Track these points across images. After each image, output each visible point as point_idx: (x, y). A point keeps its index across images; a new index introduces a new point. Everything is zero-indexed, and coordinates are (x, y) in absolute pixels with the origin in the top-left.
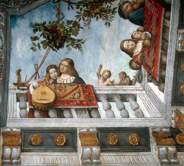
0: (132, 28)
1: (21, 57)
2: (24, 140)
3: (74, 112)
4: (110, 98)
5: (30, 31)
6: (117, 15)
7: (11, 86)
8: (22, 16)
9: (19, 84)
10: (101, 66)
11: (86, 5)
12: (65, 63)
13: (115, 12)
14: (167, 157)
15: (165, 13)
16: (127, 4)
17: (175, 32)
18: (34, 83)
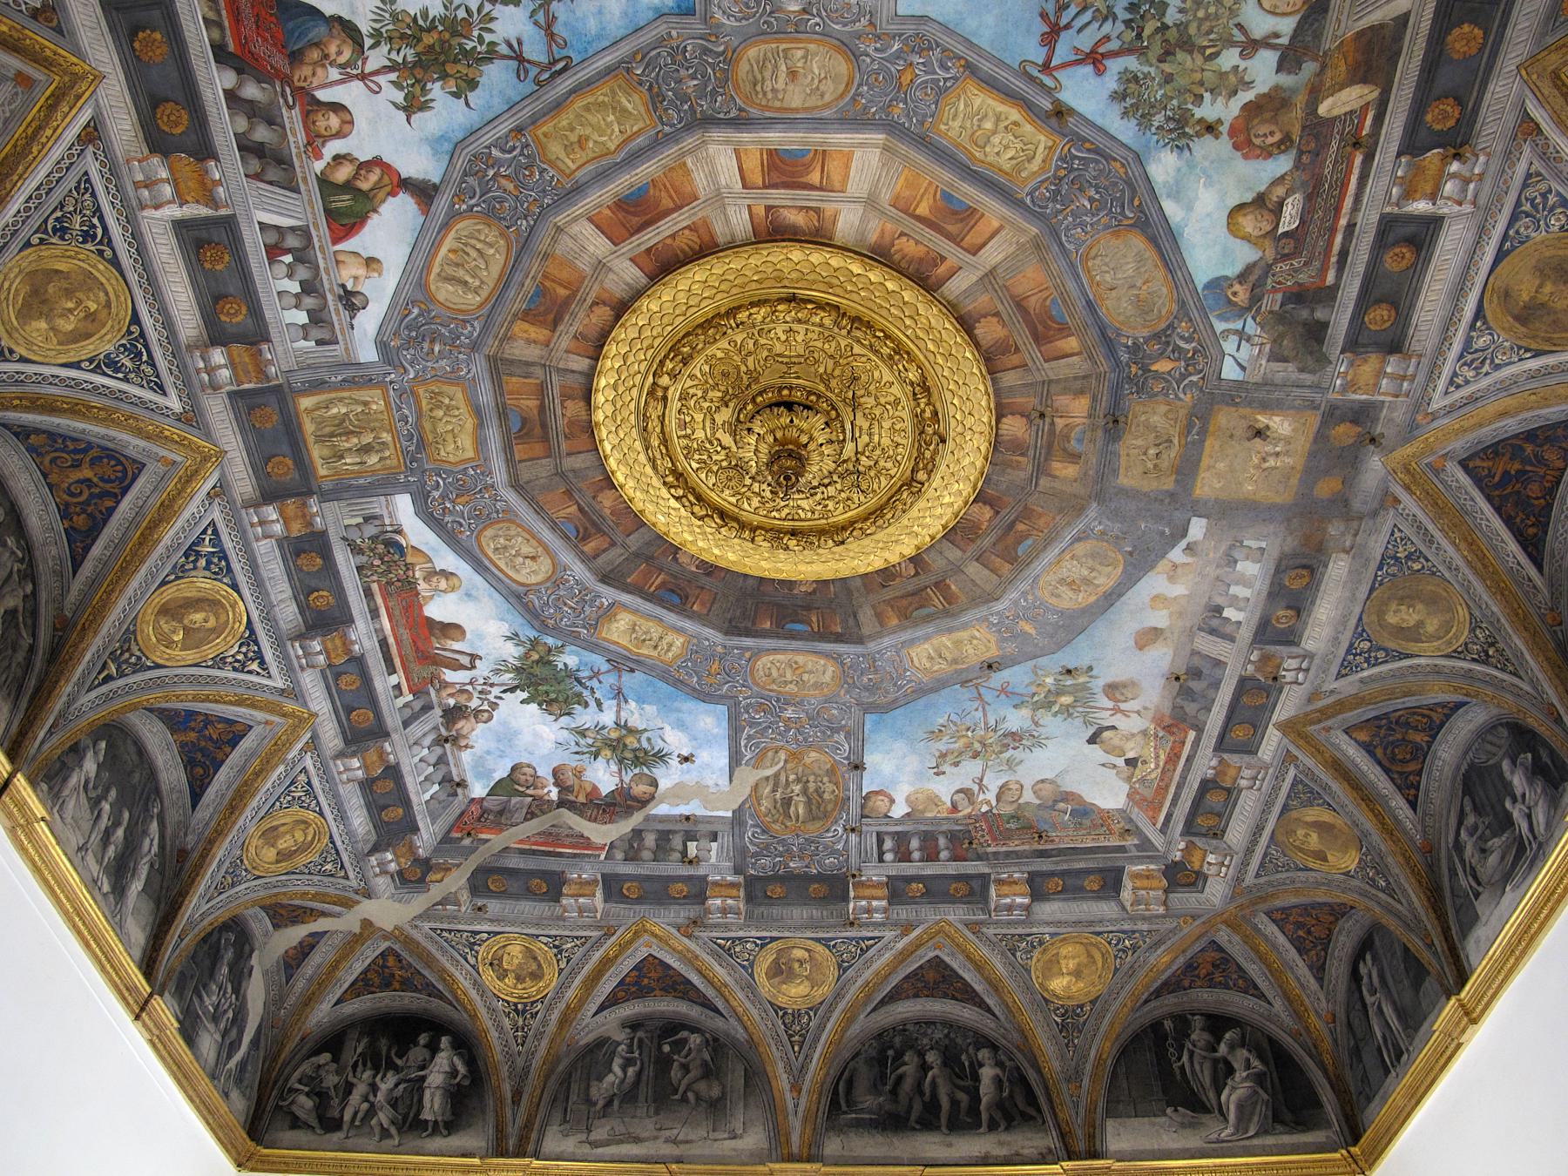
6: (365, 27)
8: (661, 15)
11: (465, 53)
13: (371, 36)
15: (223, 36)
16: (342, 60)
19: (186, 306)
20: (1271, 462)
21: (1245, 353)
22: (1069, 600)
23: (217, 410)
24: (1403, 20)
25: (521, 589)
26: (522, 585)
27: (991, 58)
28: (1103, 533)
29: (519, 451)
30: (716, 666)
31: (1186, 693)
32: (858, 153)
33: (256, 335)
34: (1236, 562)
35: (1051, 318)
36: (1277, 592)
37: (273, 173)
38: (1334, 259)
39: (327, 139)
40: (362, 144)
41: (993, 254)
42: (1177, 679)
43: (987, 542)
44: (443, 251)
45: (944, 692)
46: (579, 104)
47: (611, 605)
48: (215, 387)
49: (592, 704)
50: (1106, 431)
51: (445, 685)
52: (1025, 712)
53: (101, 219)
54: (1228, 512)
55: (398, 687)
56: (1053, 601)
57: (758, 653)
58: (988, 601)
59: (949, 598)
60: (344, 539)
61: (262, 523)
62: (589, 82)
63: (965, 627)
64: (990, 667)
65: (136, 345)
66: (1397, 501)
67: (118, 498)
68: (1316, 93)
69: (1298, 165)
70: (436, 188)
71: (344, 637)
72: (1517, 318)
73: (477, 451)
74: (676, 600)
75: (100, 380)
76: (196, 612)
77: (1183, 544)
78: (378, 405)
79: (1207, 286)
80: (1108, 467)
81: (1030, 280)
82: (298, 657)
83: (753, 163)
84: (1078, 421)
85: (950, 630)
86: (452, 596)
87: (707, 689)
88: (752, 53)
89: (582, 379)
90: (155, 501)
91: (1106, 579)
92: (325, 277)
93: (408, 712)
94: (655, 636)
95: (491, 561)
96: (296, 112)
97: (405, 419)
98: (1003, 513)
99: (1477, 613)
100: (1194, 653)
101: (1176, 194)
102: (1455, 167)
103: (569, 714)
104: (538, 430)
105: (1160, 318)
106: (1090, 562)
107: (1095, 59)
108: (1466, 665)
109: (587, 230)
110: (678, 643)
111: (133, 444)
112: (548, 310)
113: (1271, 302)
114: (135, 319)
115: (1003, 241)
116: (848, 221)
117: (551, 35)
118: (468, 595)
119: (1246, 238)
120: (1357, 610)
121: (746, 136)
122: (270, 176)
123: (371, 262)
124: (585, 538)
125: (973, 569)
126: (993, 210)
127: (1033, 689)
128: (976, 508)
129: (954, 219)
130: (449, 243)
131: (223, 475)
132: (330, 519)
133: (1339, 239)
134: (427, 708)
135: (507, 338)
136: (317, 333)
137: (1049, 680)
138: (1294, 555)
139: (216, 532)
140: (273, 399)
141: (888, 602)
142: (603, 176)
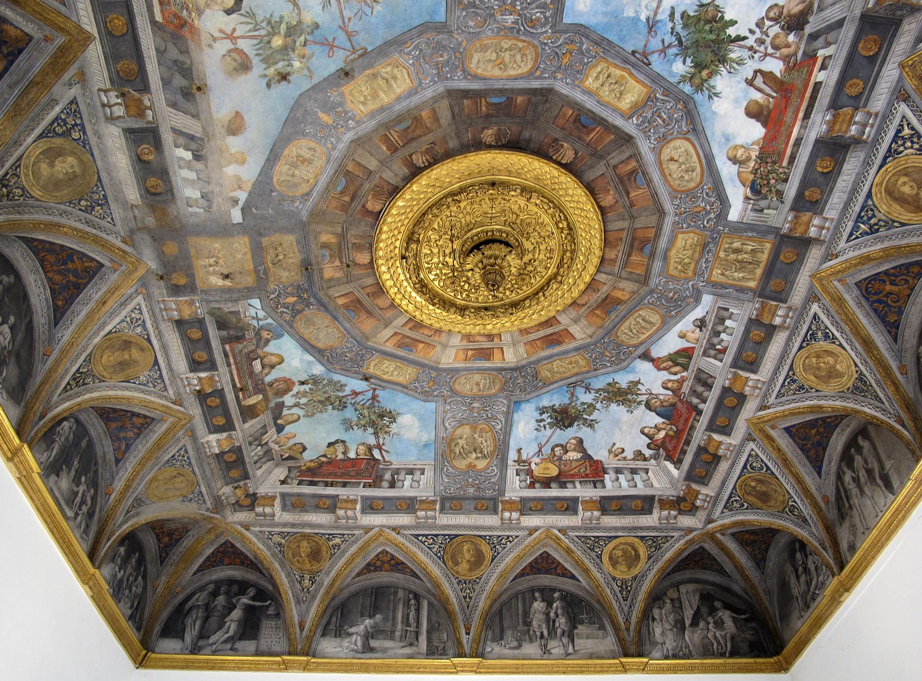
0: (659, 420)
1: (522, 436)
2: (524, 506)
3: (578, 484)
4: (618, 471)
5: (536, 415)
6: (643, 407)
7: (510, 462)
8: (528, 401)
9: (519, 461)
10: (614, 444)
11: (608, 392)
12: (574, 441)
14: (667, 519)
17: (701, 432)
18: (536, 460)
19: (776, 344)
20: (212, 261)
21: (252, 312)
22: (299, 148)
23: (798, 296)
24: (244, 422)
25: (690, 136)
26: (688, 140)
27: (397, 390)
28: (293, 201)
29: (651, 234)
30: (566, 60)
31: (186, 71)
32: (451, 361)
33: (753, 323)
34: (202, 197)
35: (354, 311)
36: (164, 173)
37: (704, 376)
38: (230, 354)
39: (677, 381)
40: (664, 376)
41: (387, 333)
42: (199, 89)
43: (367, 186)
44: (647, 334)
45: (379, 42)
46: (568, 374)
47: (631, 117)
48: (790, 308)
49: (677, 16)
50: (310, 264)
51: (785, 59)
52: (308, 18)
53: (784, 383)
54: (225, 230)
55: (823, 67)
56: (312, 145)
57: (530, 75)
58: (359, 139)
59: (386, 139)
60: (782, 202)
61: (822, 228)
62: (562, 380)
63: (372, 115)
64: (347, 74)
65: (810, 337)
66: (125, 242)
67: (886, 273)
68: (266, 399)
69: (262, 380)
70: (639, 357)
71: (830, 129)
72: (130, 342)
73: (676, 237)
74: (583, 119)
75: (837, 334)
76: (904, 193)
77: (241, 204)
78: (717, 272)
79: (283, 335)
80: (304, 243)
81: (367, 325)
82: (872, 126)
83: (497, 354)
84: (328, 266)
85: (382, 109)
86: (739, 141)
87: (577, 39)
88: (493, 391)
89: (602, 269)
90: (866, 267)
91: (281, 170)
92: (707, 337)
93: (831, 37)
94: (606, 88)
95: (700, 162)
96: (683, 390)
97: (707, 261)
98: (359, 207)
99: (31, 201)
100: (196, 116)
101: (309, 362)
102: (198, 388)
103: (702, 6)
104: (636, 245)
105: (300, 320)
106: (296, 180)
107: (355, 393)
108: (8, 165)
109: (577, 335)
110: (590, 80)
111: (850, 299)
112: (608, 304)
113: (249, 334)
114: (801, 347)
115: (384, 338)
116: (456, 341)
117: (573, 395)
118: (728, 140)
119: (272, 354)
120: (99, 163)
121: (499, 365)
122: (706, 376)
123: (682, 336)
124: (634, 172)
125: (373, 164)
126: (389, 347)
127: (308, 51)
128: (378, 208)
129: (407, 343)
130: (643, 337)
131: (821, 264)
132: (783, 217)
133: (232, 361)
134: (813, 37)
135: (633, 293)
136: (726, 314)
137: (297, 64)
138: (165, 202)
139: (851, 234)
140: (767, 292)
141: (430, 131)
142: (566, 352)
